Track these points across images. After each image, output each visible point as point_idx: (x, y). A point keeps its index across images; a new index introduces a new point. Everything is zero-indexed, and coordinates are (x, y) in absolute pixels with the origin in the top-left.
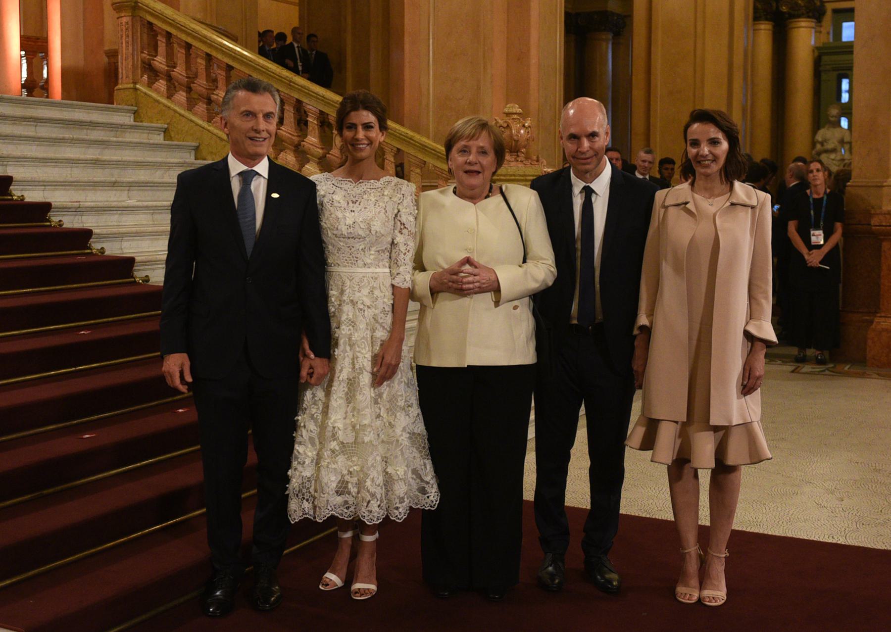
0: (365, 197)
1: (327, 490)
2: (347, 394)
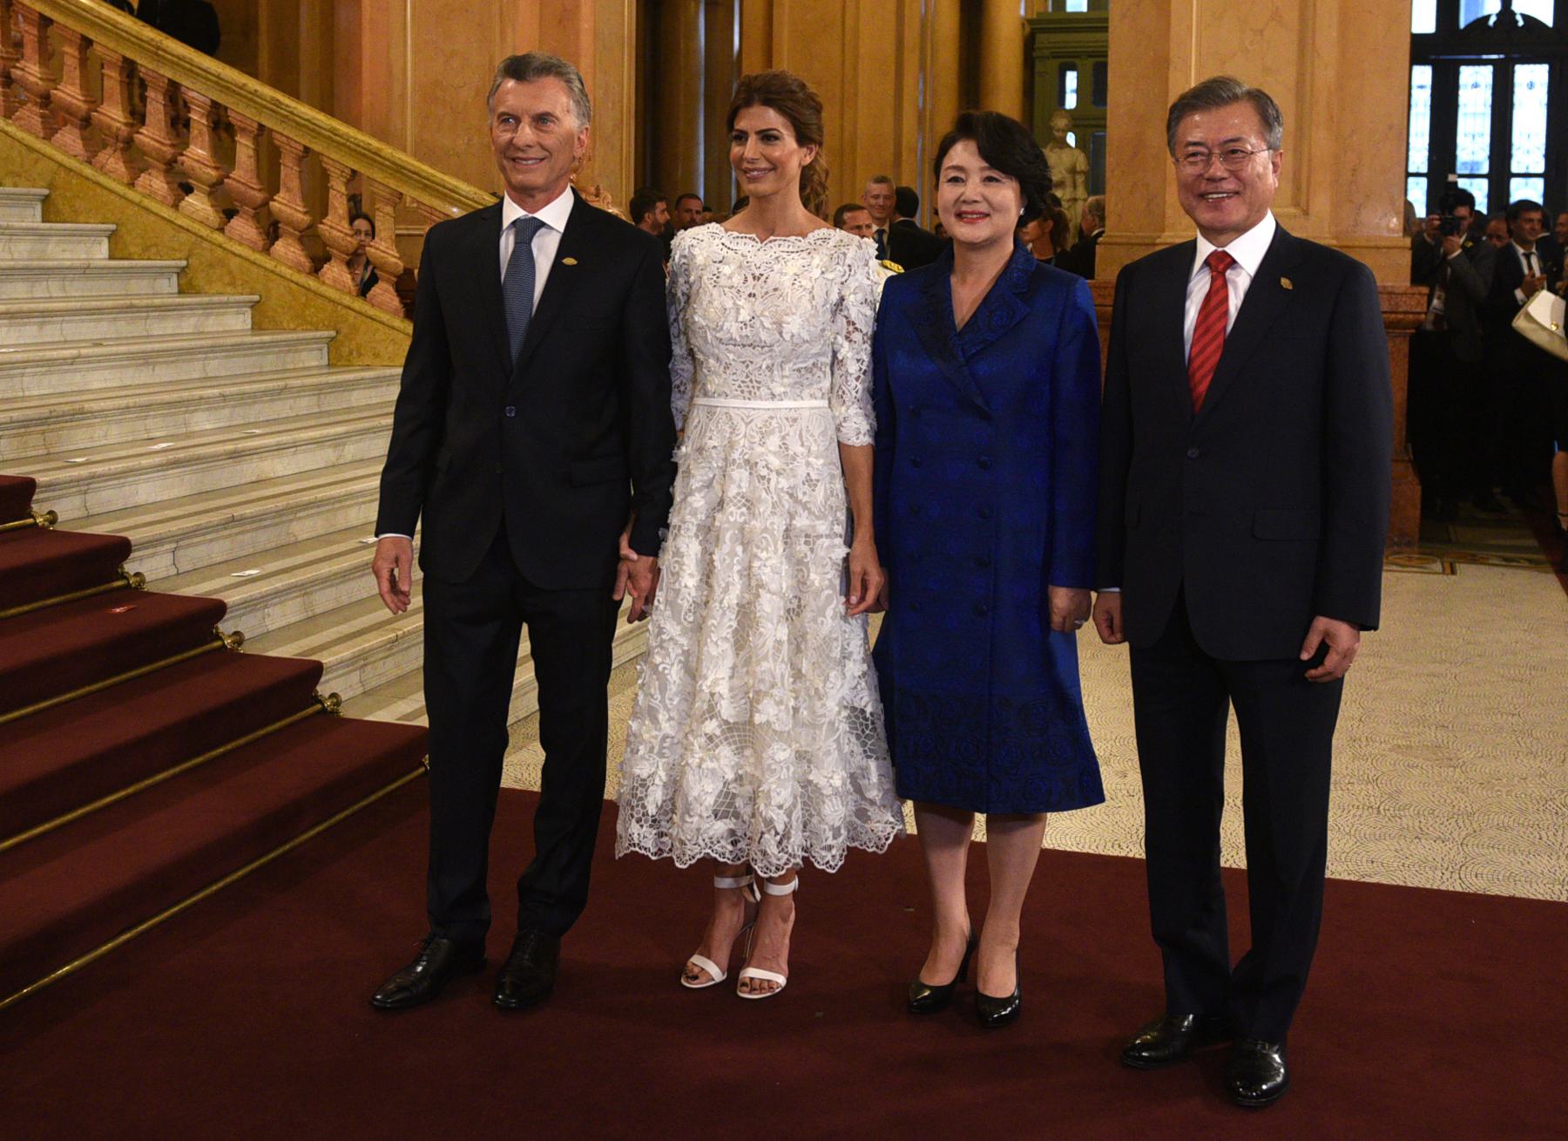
0: (777, 267)
1: (697, 809)
2: (736, 632)
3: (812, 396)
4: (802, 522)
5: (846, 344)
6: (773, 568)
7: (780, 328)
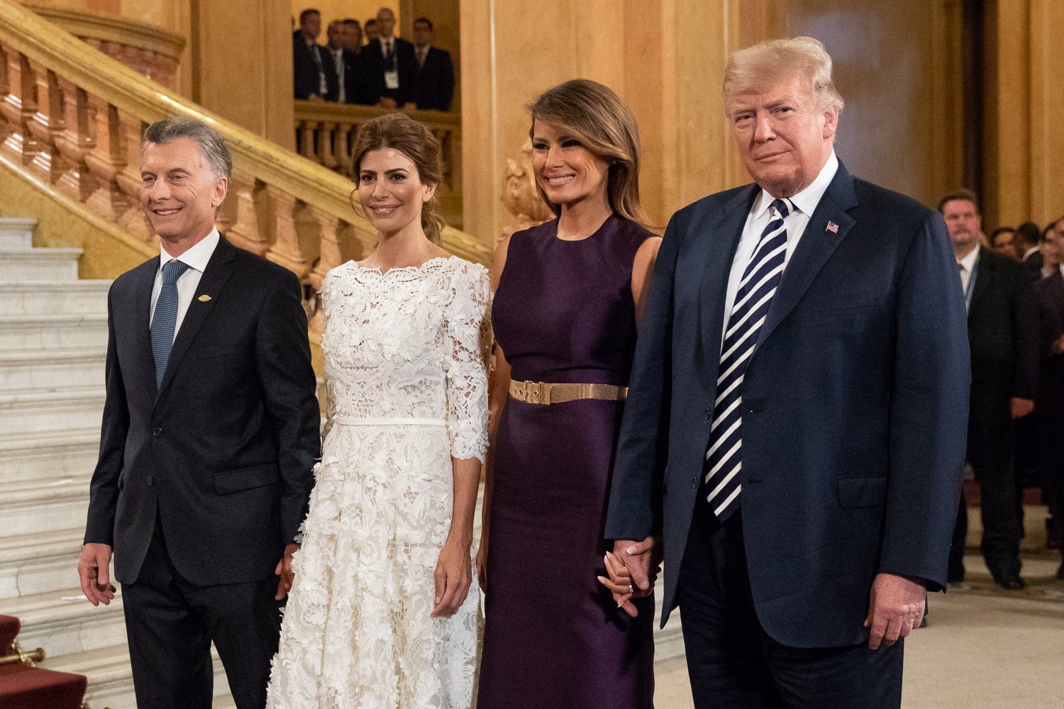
3: (423, 414)
4: (402, 531)
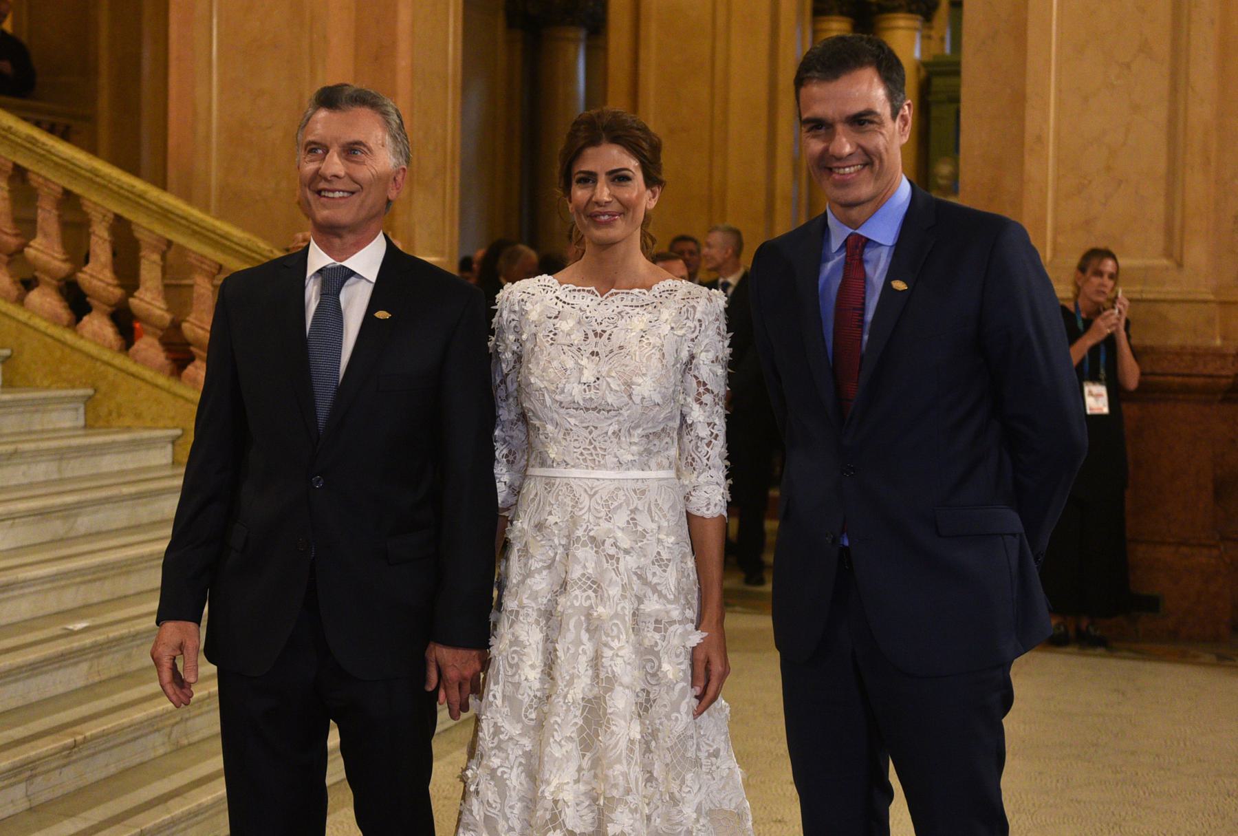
0: (621, 323)
4: (652, 605)
5: (696, 407)
6: (621, 659)
7: (617, 383)
